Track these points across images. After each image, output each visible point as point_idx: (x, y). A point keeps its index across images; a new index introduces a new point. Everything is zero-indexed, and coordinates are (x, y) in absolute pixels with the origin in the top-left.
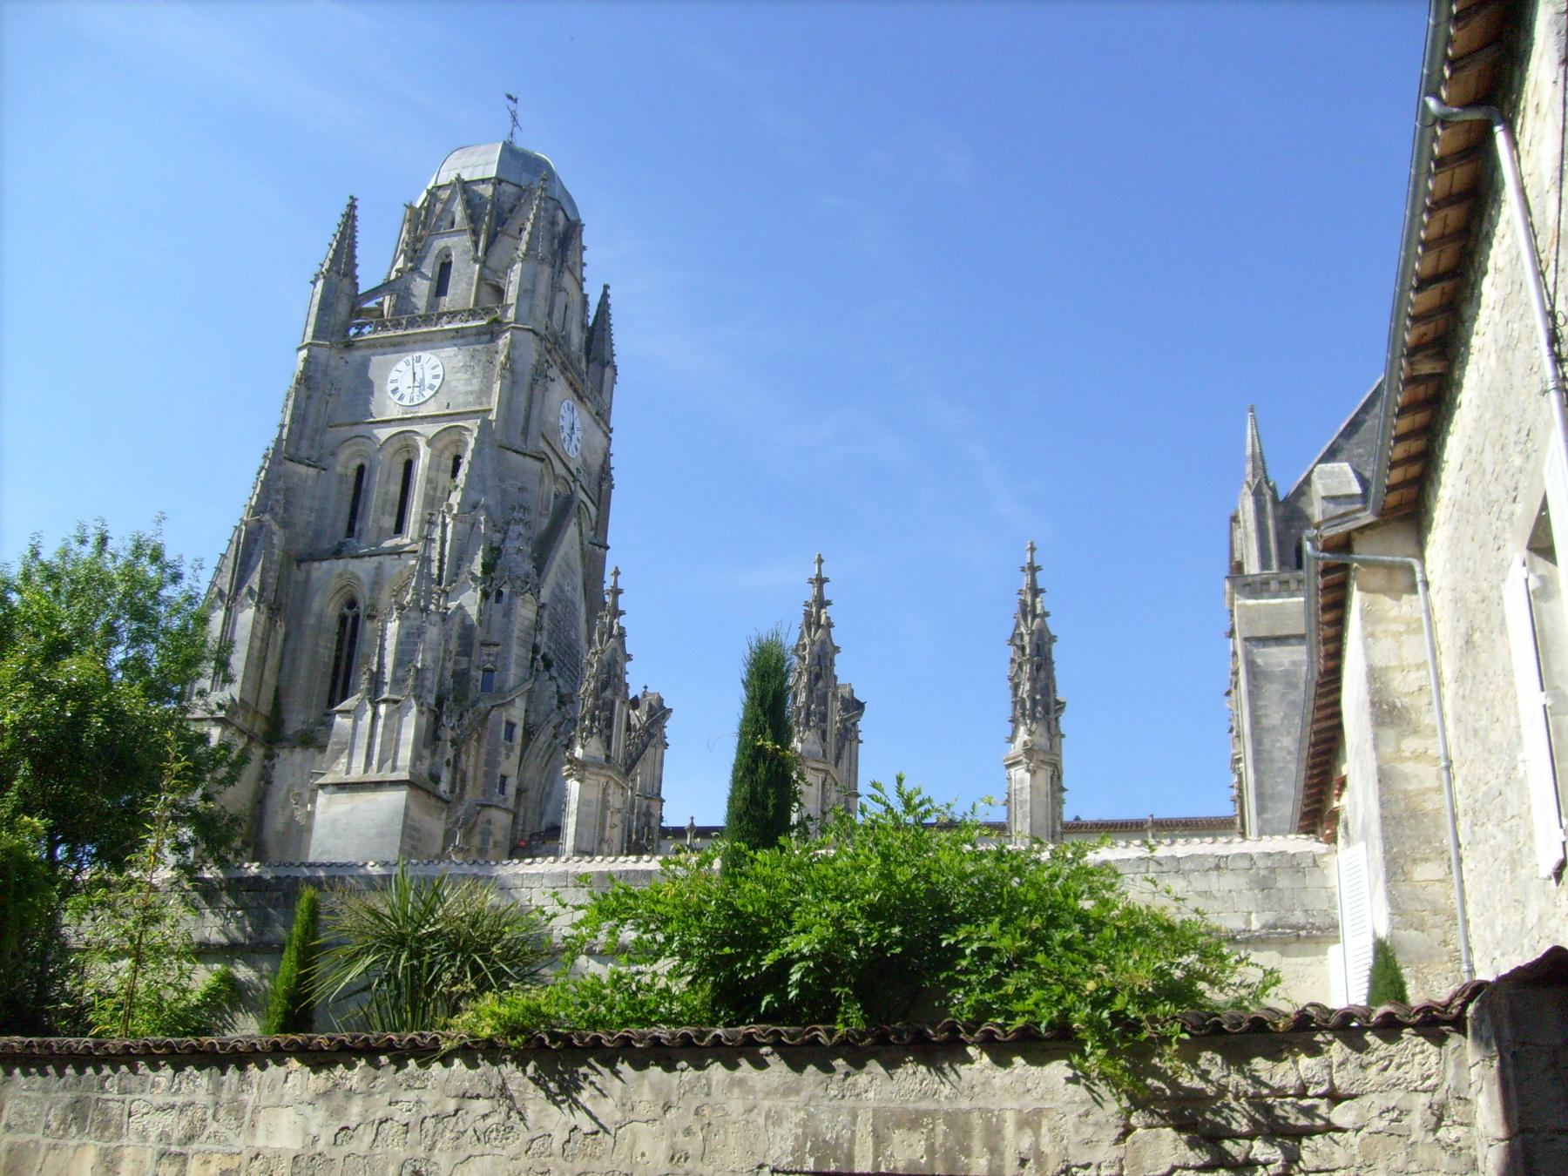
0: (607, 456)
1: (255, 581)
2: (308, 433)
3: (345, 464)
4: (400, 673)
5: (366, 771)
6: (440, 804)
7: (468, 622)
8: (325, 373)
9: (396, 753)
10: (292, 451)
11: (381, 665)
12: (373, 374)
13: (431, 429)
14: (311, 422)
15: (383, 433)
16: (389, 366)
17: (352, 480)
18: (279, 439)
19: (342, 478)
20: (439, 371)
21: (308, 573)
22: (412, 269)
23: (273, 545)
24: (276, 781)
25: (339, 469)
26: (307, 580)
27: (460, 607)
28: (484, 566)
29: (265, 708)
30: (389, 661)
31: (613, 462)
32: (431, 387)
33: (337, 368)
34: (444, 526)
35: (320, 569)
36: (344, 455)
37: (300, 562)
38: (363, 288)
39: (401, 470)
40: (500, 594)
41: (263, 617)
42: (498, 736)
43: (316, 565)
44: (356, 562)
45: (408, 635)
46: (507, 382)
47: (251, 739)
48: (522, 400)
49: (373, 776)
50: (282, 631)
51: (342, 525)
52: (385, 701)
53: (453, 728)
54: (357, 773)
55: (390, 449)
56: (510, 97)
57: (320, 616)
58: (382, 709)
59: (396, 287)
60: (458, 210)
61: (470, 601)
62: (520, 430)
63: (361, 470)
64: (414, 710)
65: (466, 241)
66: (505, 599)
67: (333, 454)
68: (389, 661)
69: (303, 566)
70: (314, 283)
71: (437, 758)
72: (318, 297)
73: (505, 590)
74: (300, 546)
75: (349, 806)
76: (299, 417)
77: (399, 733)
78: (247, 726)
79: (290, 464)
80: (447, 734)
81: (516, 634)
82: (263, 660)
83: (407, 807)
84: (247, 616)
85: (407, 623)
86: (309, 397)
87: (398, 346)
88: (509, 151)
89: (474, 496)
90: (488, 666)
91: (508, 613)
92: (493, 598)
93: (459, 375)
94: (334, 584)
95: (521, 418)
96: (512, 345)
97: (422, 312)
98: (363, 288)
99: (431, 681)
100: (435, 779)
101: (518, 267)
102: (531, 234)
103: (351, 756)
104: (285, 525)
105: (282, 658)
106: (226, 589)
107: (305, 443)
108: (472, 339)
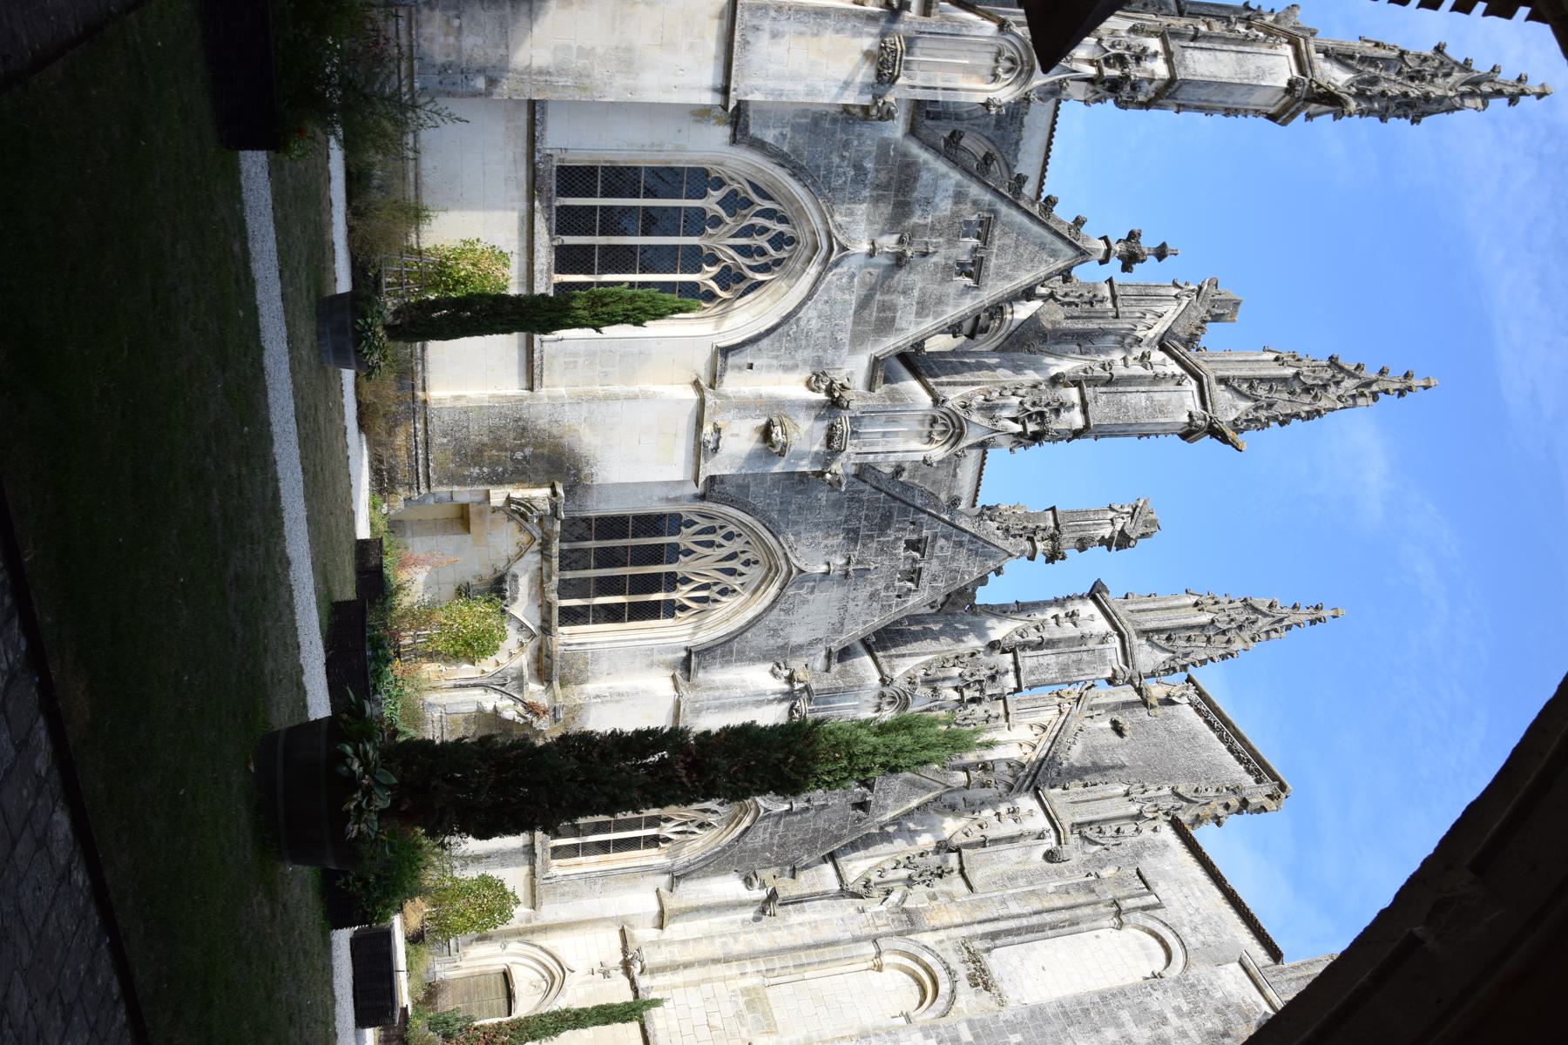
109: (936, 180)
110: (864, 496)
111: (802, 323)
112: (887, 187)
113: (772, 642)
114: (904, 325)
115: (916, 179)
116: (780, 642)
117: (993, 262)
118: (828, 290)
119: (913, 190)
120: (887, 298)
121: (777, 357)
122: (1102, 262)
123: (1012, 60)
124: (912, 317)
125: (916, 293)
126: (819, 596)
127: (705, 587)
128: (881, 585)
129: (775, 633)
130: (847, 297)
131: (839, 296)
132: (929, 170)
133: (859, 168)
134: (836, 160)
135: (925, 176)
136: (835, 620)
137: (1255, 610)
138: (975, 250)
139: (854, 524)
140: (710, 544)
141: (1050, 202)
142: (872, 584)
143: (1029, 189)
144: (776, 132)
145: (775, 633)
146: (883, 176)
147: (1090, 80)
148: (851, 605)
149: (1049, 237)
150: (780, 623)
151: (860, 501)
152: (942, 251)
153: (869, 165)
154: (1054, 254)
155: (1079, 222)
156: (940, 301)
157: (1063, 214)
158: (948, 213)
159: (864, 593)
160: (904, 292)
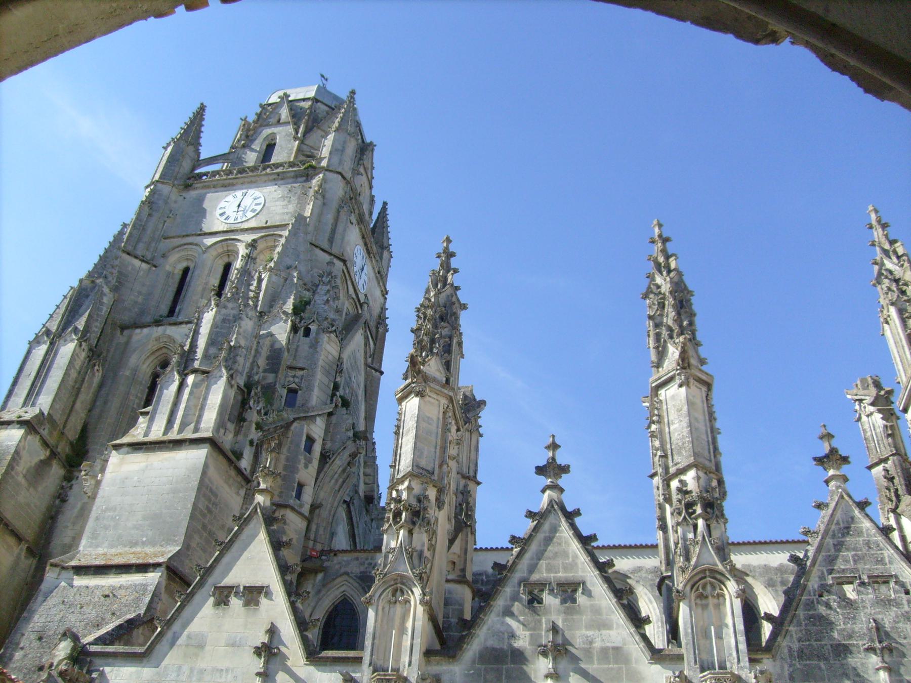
0: (383, 309)
1: (81, 324)
2: (146, 239)
3: (174, 264)
4: (213, 351)
5: (165, 433)
6: (239, 479)
7: (277, 346)
8: (166, 203)
9: (200, 417)
10: (130, 248)
11: (193, 345)
12: (206, 205)
13: (249, 238)
14: (149, 232)
15: (209, 241)
16: (219, 200)
17: (178, 277)
18: (121, 233)
19: (169, 275)
20: (262, 200)
21: (130, 337)
22: (244, 146)
23: (102, 304)
24: (71, 500)
25: (168, 268)
26: (127, 343)
27: (271, 335)
28: (294, 305)
29: (72, 433)
30: (202, 343)
31: (388, 314)
32: (253, 211)
33: (176, 202)
34: (260, 280)
35: (140, 335)
36: (173, 258)
37: (123, 328)
38: (205, 154)
39: (220, 270)
40: (307, 332)
41: (83, 355)
42: (298, 445)
43: (138, 331)
44: (174, 328)
45: (224, 321)
46: (319, 202)
47: (53, 454)
48: (329, 218)
49: (173, 435)
50: (98, 376)
51: (164, 309)
52: (195, 371)
53: (259, 412)
54: (157, 432)
55: (213, 252)
56: (322, 76)
57: (135, 371)
58: (191, 379)
59: (232, 157)
60: (284, 113)
61: (281, 331)
62: (327, 235)
63: (186, 271)
64: (224, 379)
65: (290, 129)
66: (313, 334)
67: (164, 256)
68: (202, 343)
69: (126, 332)
70: (165, 148)
71: (240, 437)
72: (165, 158)
73: (313, 327)
74: (126, 318)
75: (143, 465)
76: (140, 224)
77: (205, 399)
78: (52, 441)
79: (125, 256)
80: (253, 417)
81: (321, 363)
82: (77, 392)
83: (206, 465)
84: (67, 349)
85: (224, 311)
86: (150, 215)
87: (228, 186)
88: (321, 90)
89: (289, 261)
90: (293, 386)
91: (314, 345)
92: (301, 331)
93: (278, 203)
94: (152, 346)
95: (329, 228)
96: (324, 180)
97: (251, 164)
98: (205, 154)
99: (243, 363)
100: (239, 456)
101: (331, 137)
102: (342, 119)
103: (151, 421)
104: (115, 289)
105: (94, 401)
106: (54, 329)
107: (141, 246)
108: (291, 180)
117: (562, 575)
119: (502, 649)
122: (562, 490)
123: (395, 591)
125: (590, 633)
132: (486, 640)
135: (492, 643)
137: (880, 274)
138: (551, 591)
141: (514, 540)
143: (502, 559)
147: (410, 532)
149: (540, 536)
152: (553, 617)
154: (555, 529)
155: (530, 515)
157: (524, 527)
160: (591, 643)
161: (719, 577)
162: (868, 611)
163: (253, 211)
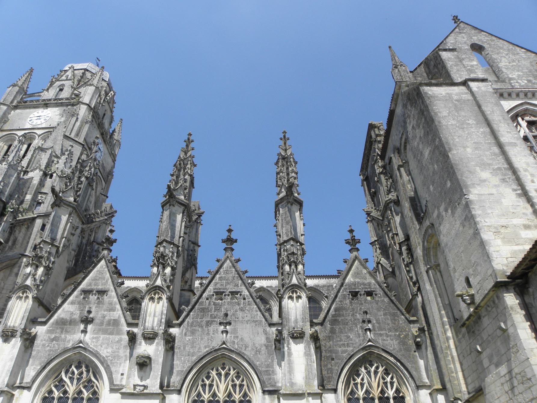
31: (114, 170)
109: (64, 312)
110: (191, 321)
111: (108, 355)
112: (62, 329)
113: (263, 352)
114: (117, 316)
115: (63, 319)
116: (264, 348)
117: (100, 287)
118: (96, 346)
119: (66, 319)
120: (105, 324)
121: (120, 364)
124: (115, 313)
125: (106, 313)
126: (240, 333)
127: (234, 386)
128: (237, 307)
129: (258, 351)
130: (101, 339)
131: (100, 342)
133: (53, 340)
134: (48, 348)
135: (62, 316)
136: (254, 324)
139: (204, 323)
140: (211, 386)
142: (236, 311)
144: (32, 371)
145: (258, 351)
146: (59, 331)
148: (246, 319)
150: (253, 349)
151: (193, 323)
153: (53, 336)
156: (111, 304)
158: (78, 306)
159: (240, 314)
160: (104, 317)
161: (161, 290)
162: (226, 307)
163: (45, 120)
